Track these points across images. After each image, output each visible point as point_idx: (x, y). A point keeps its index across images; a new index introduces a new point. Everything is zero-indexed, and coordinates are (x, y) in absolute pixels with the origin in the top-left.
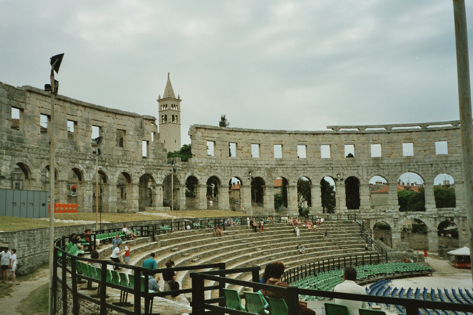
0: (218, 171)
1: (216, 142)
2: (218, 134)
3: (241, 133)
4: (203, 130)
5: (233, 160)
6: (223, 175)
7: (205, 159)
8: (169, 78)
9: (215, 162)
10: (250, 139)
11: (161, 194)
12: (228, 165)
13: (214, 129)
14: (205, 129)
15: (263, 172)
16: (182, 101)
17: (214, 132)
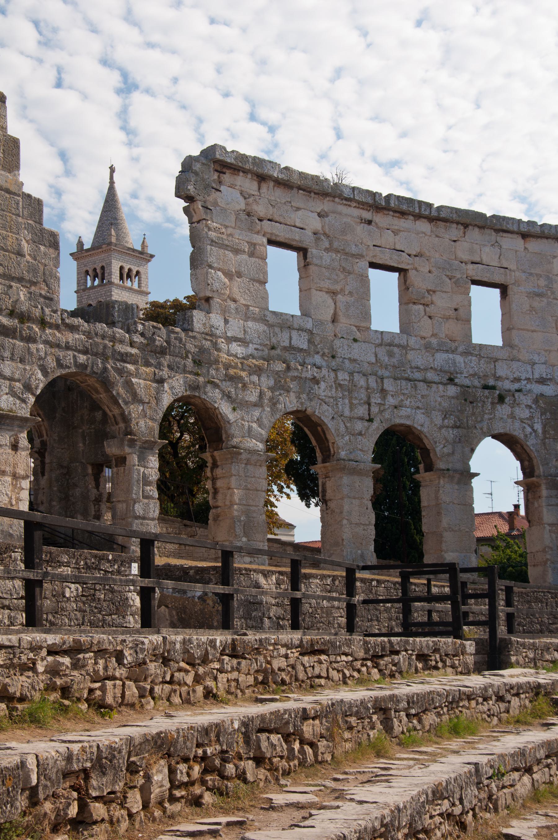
0: (322, 390)
1: (313, 251)
2: (319, 215)
3: (424, 226)
4: (250, 185)
5: (390, 345)
6: (347, 413)
7: (261, 327)
8: (112, 182)
9: (305, 346)
10: (465, 257)
11: (21, 472)
12: (366, 368)
13: (299, 188)
14: (262, 178)
15: (526, 414)
16: (153, 259)
17: (299, 199)
